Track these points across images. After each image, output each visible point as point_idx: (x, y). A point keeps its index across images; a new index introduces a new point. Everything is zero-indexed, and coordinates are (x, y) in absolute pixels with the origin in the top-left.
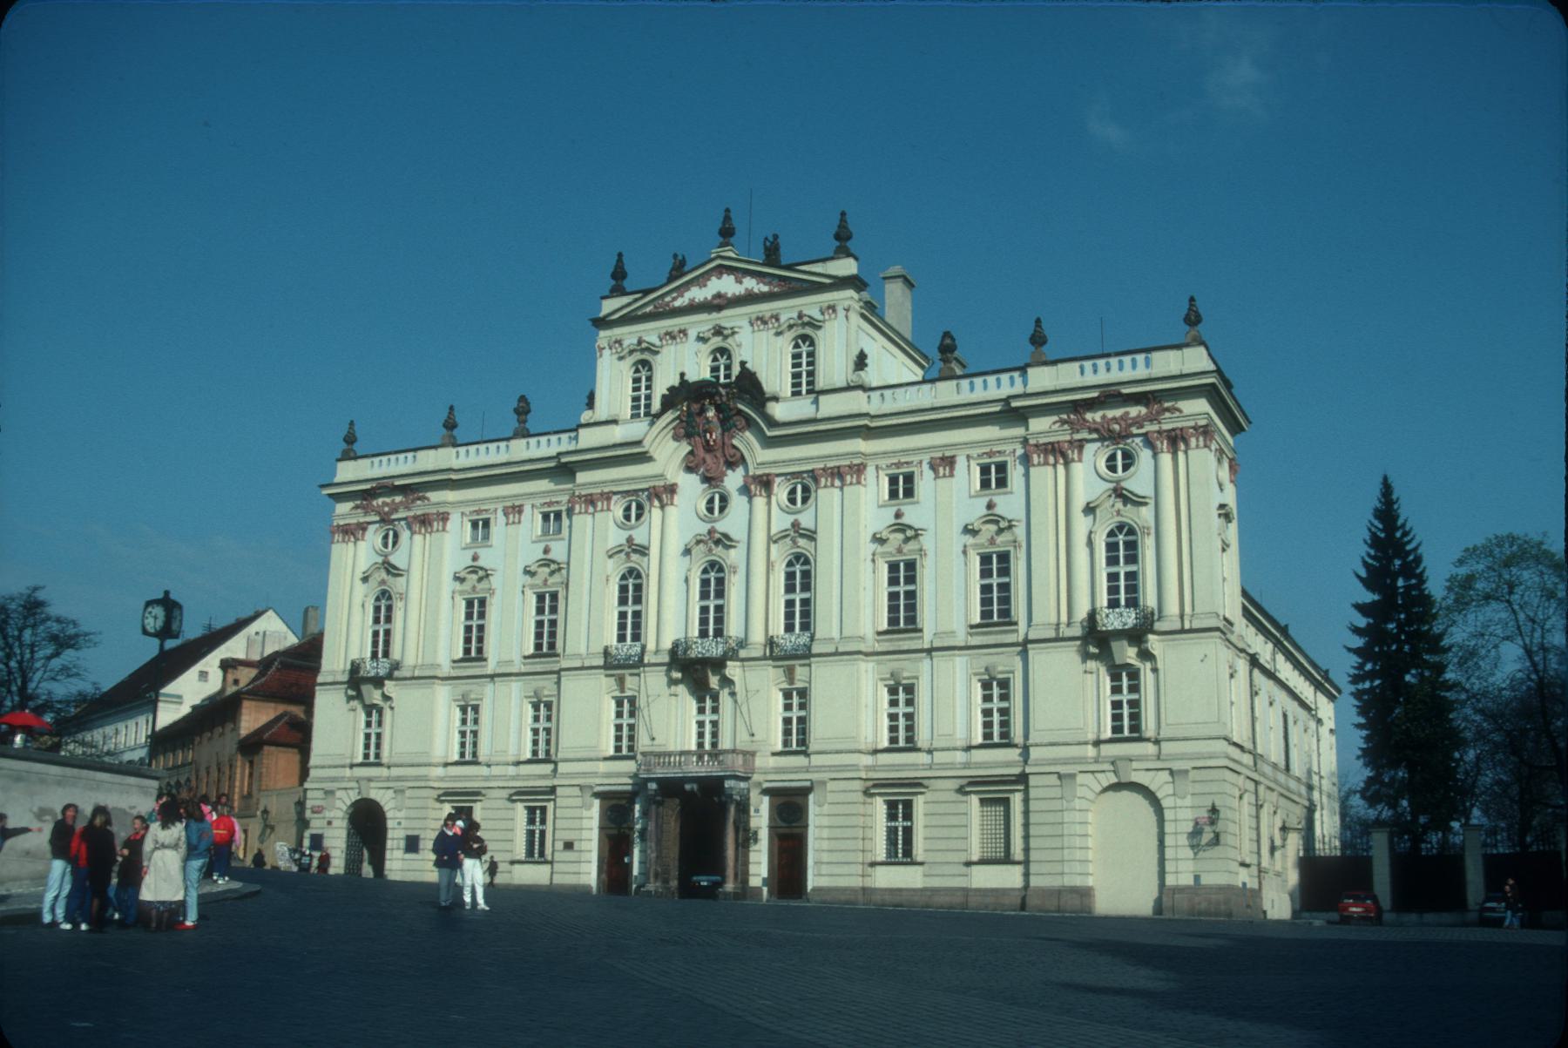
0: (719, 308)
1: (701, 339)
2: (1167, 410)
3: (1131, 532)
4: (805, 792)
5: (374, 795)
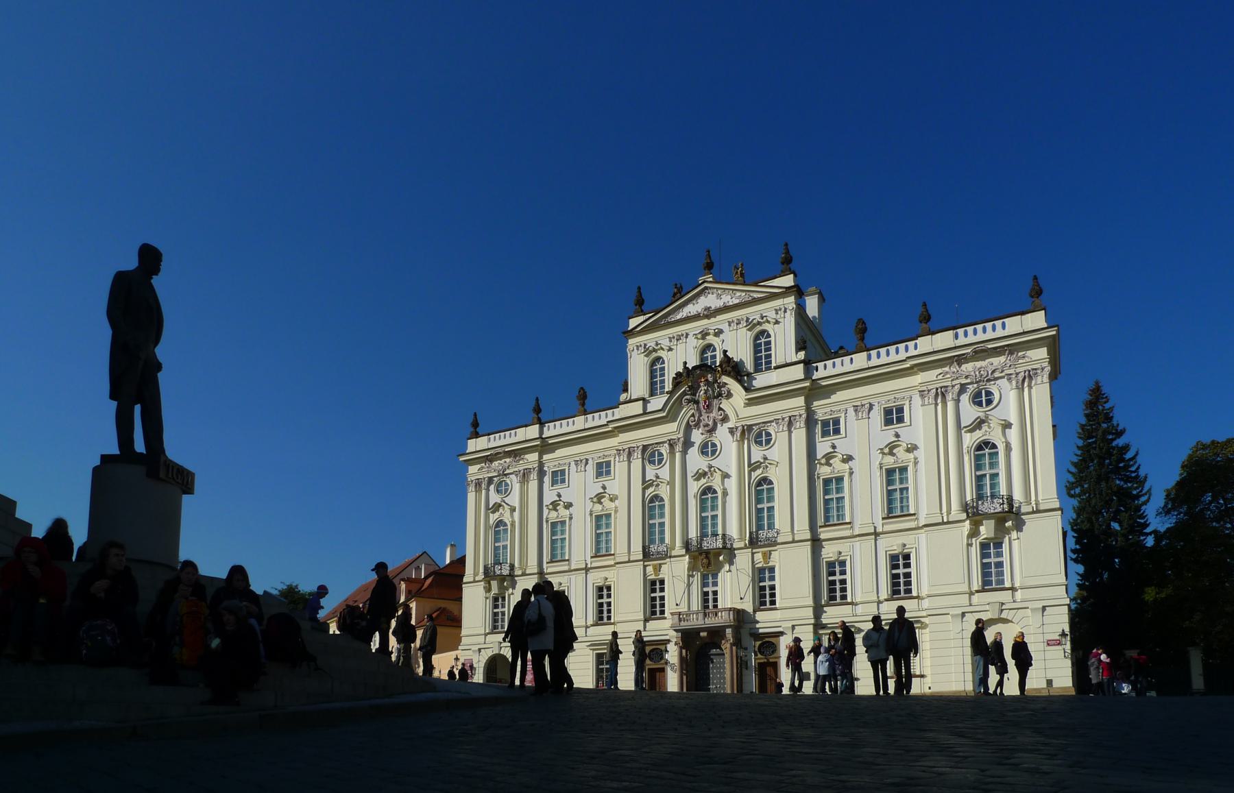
0: (708, 317)
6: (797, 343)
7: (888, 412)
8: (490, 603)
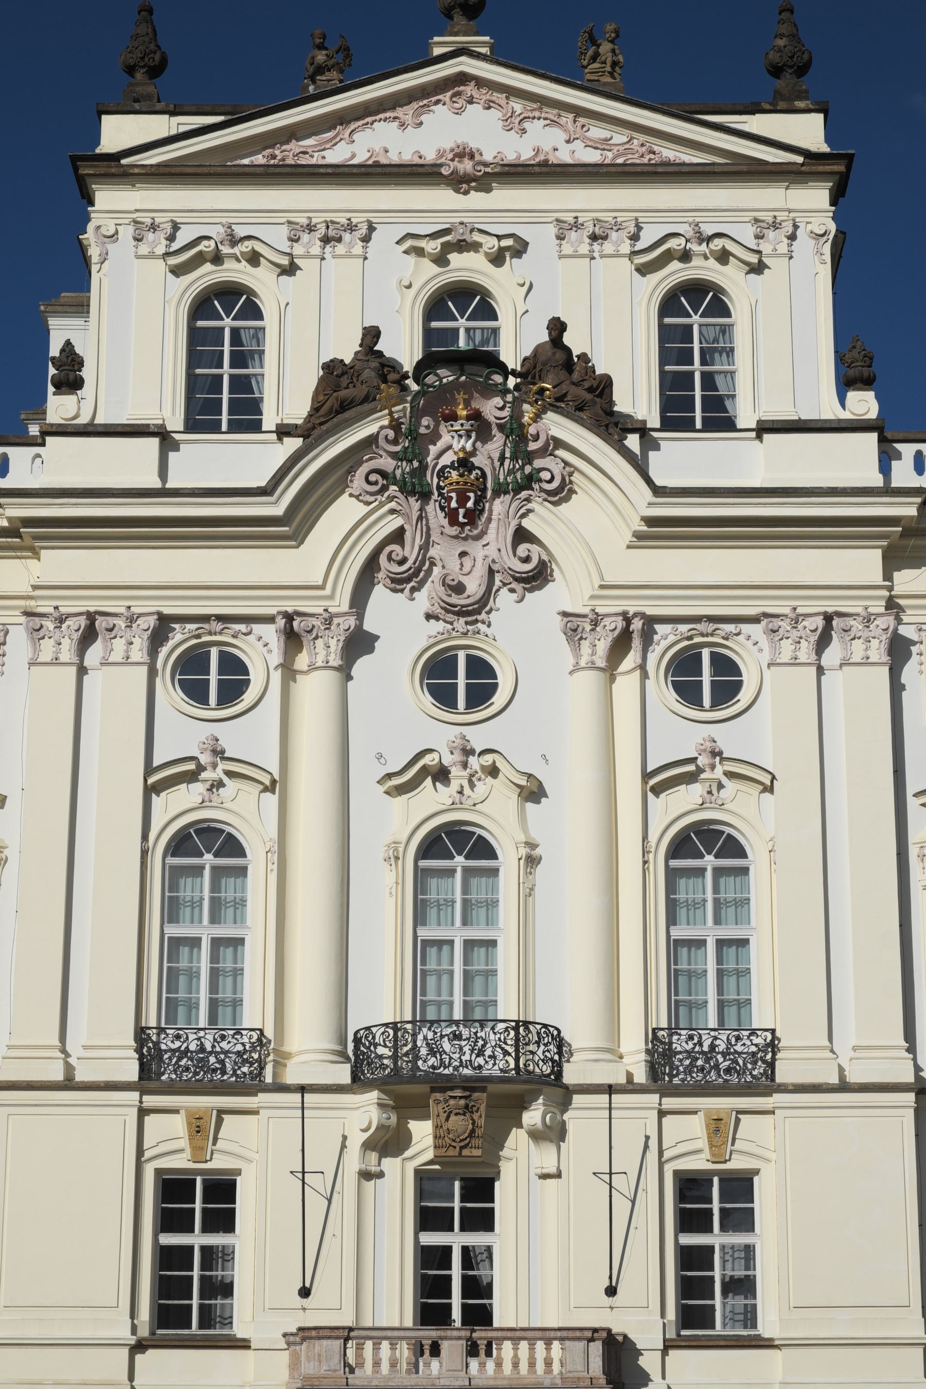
6: (840, 358)
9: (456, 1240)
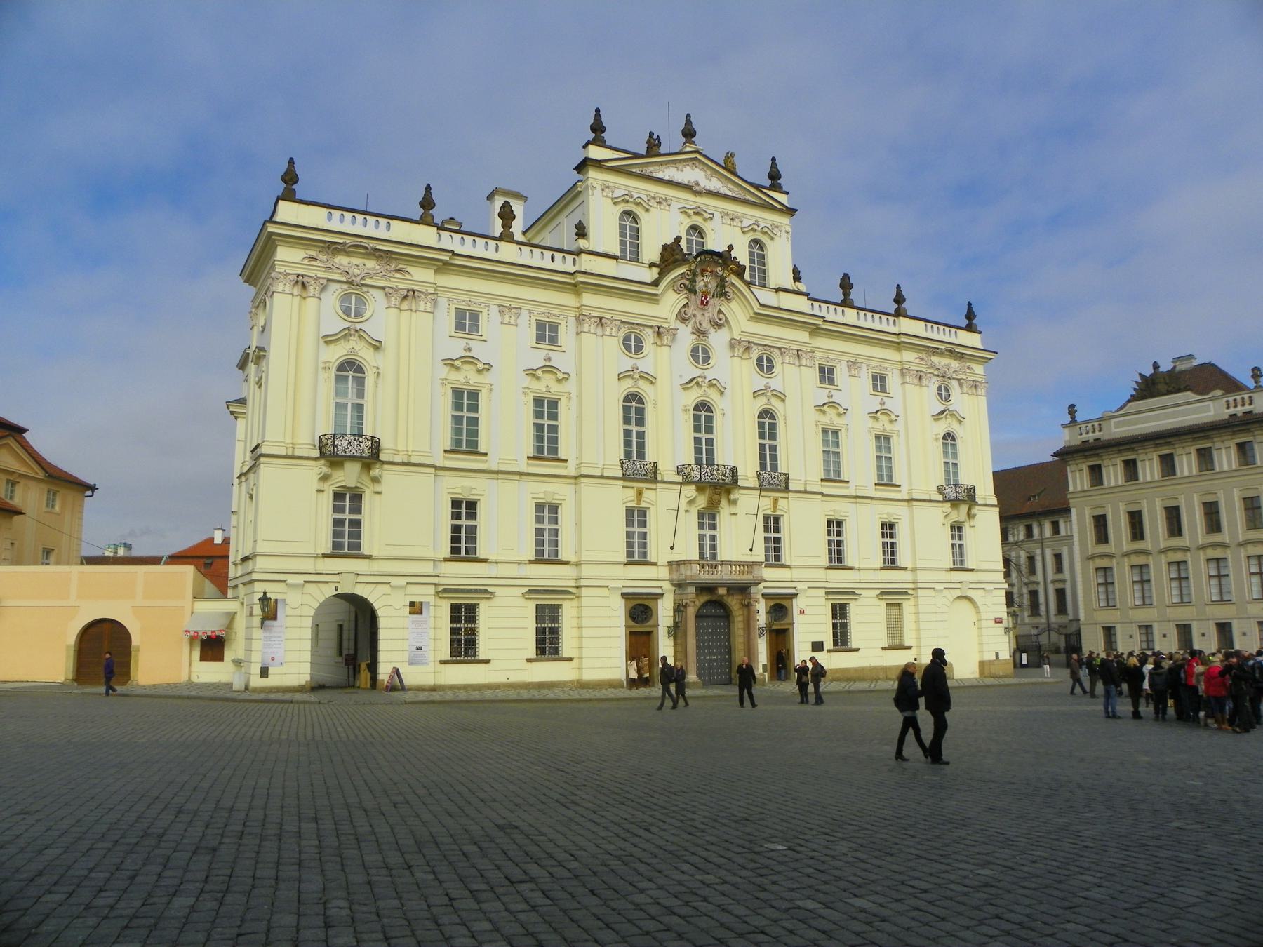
0: (698, 193)
1: (684, 211)
2: (969, 368)
3: (953, 439)
4: (793, 596)
5: (360, 591)
7: (874, 378)
8: (327, 500)
9: (708, 532)
